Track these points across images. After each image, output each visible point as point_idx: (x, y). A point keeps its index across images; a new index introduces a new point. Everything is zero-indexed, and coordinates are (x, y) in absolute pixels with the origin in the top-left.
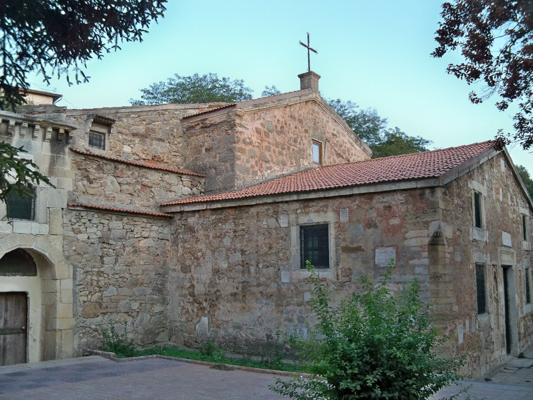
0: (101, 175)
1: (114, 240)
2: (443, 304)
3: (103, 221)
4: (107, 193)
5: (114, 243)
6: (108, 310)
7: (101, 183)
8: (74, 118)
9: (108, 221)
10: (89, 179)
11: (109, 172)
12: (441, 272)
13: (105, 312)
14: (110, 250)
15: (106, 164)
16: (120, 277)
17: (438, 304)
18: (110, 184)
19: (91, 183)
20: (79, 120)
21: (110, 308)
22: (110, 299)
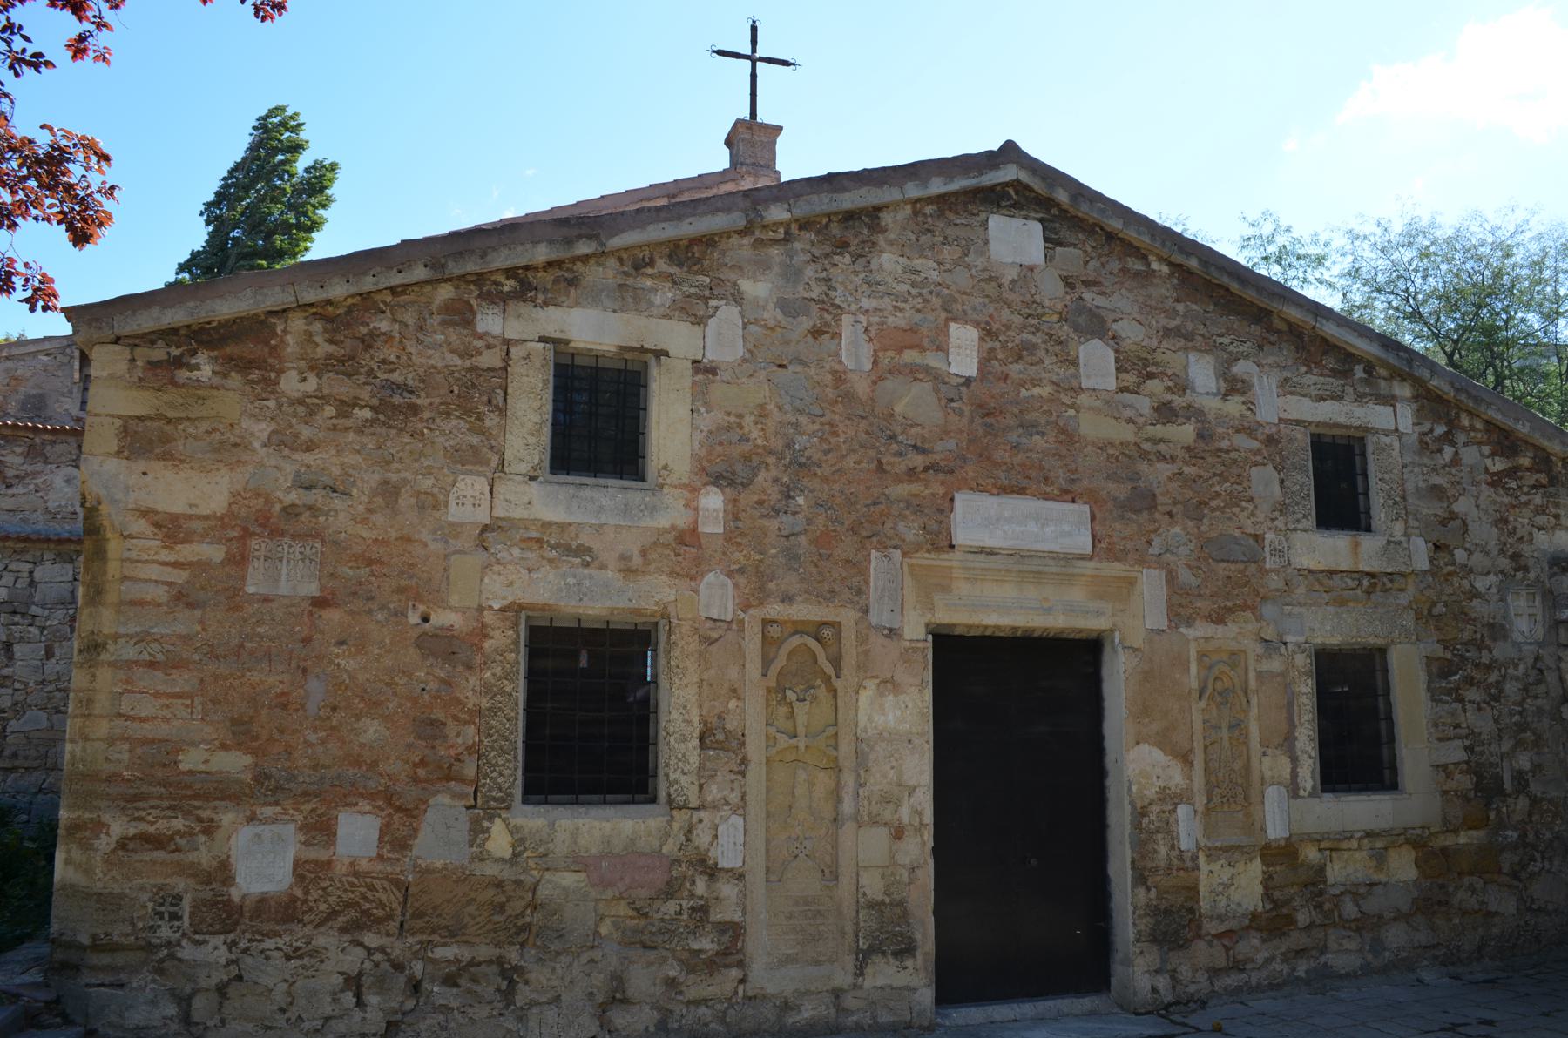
0: (39, 467)
1: (43, 606)
2: (98, 739)
3: (12, 567)
4: (52, 505)
5: (46, 612)
6: (17, 763)
7: (36, 485)
8: (48, 355)
9: (31, 566)
10: (5, 477)
11: (64, 459)
12: (106, 631)
13: (10, 766)
14: (31, 629)
15: (55, 442)
16: (59, 690)
17: (87, 739)
18: (63, 484)
19: (9, 486)
20: (60, 357)
21: (26, 758)
22: (28, 738)
